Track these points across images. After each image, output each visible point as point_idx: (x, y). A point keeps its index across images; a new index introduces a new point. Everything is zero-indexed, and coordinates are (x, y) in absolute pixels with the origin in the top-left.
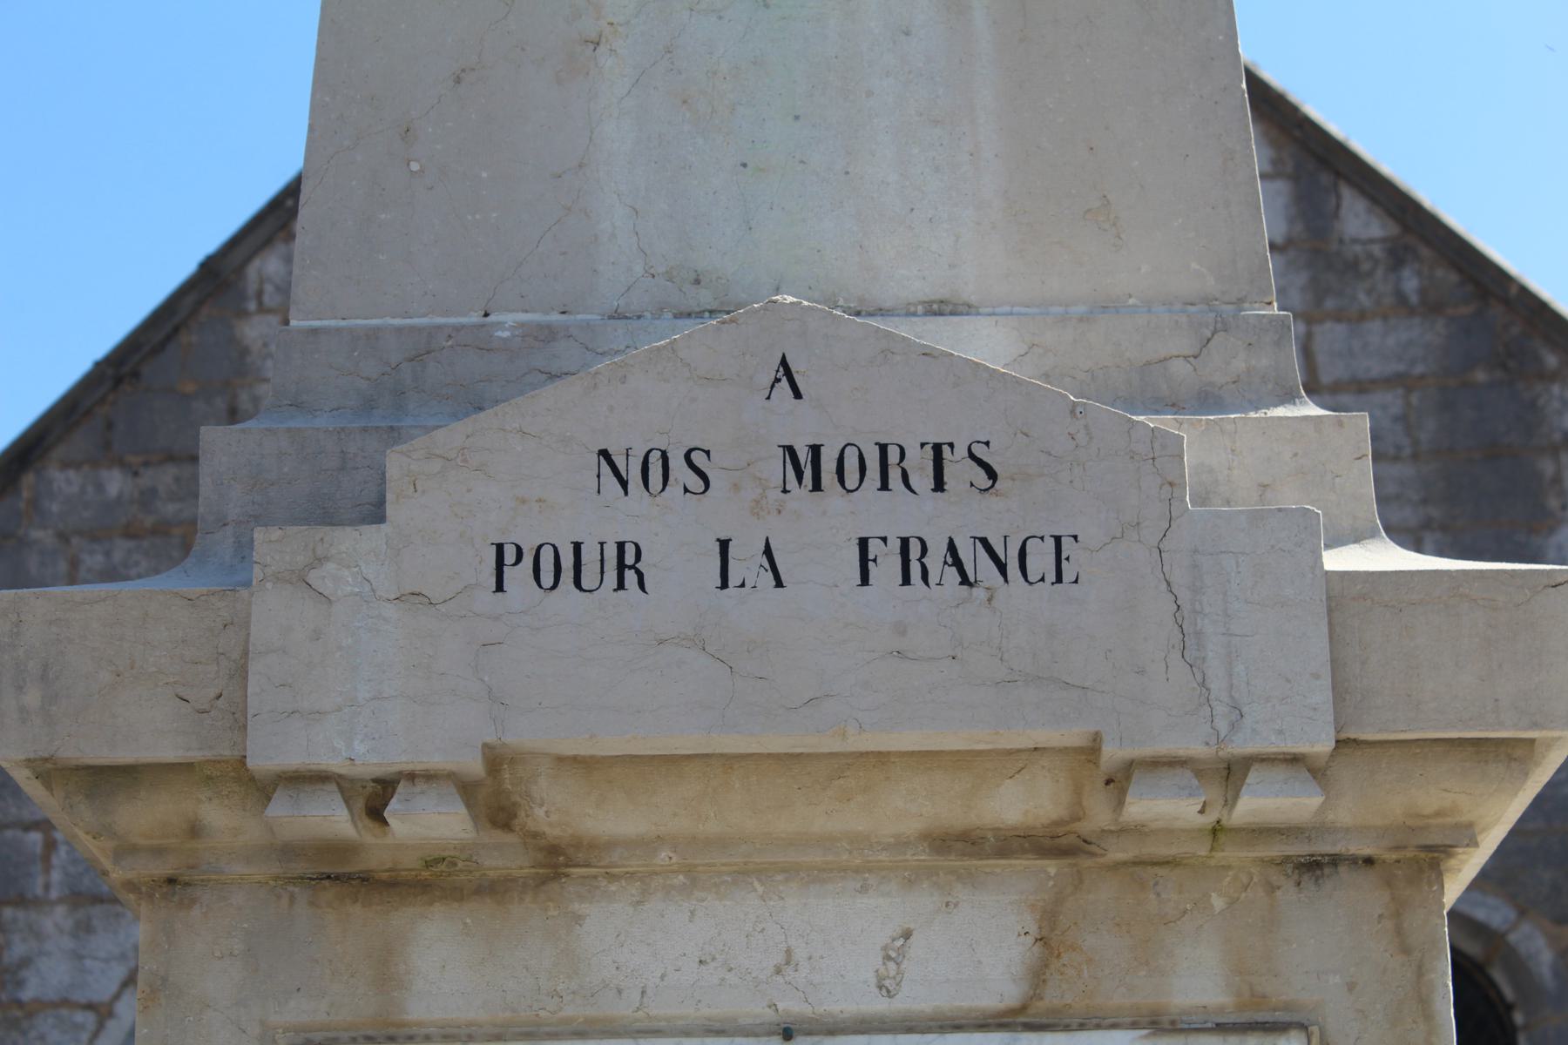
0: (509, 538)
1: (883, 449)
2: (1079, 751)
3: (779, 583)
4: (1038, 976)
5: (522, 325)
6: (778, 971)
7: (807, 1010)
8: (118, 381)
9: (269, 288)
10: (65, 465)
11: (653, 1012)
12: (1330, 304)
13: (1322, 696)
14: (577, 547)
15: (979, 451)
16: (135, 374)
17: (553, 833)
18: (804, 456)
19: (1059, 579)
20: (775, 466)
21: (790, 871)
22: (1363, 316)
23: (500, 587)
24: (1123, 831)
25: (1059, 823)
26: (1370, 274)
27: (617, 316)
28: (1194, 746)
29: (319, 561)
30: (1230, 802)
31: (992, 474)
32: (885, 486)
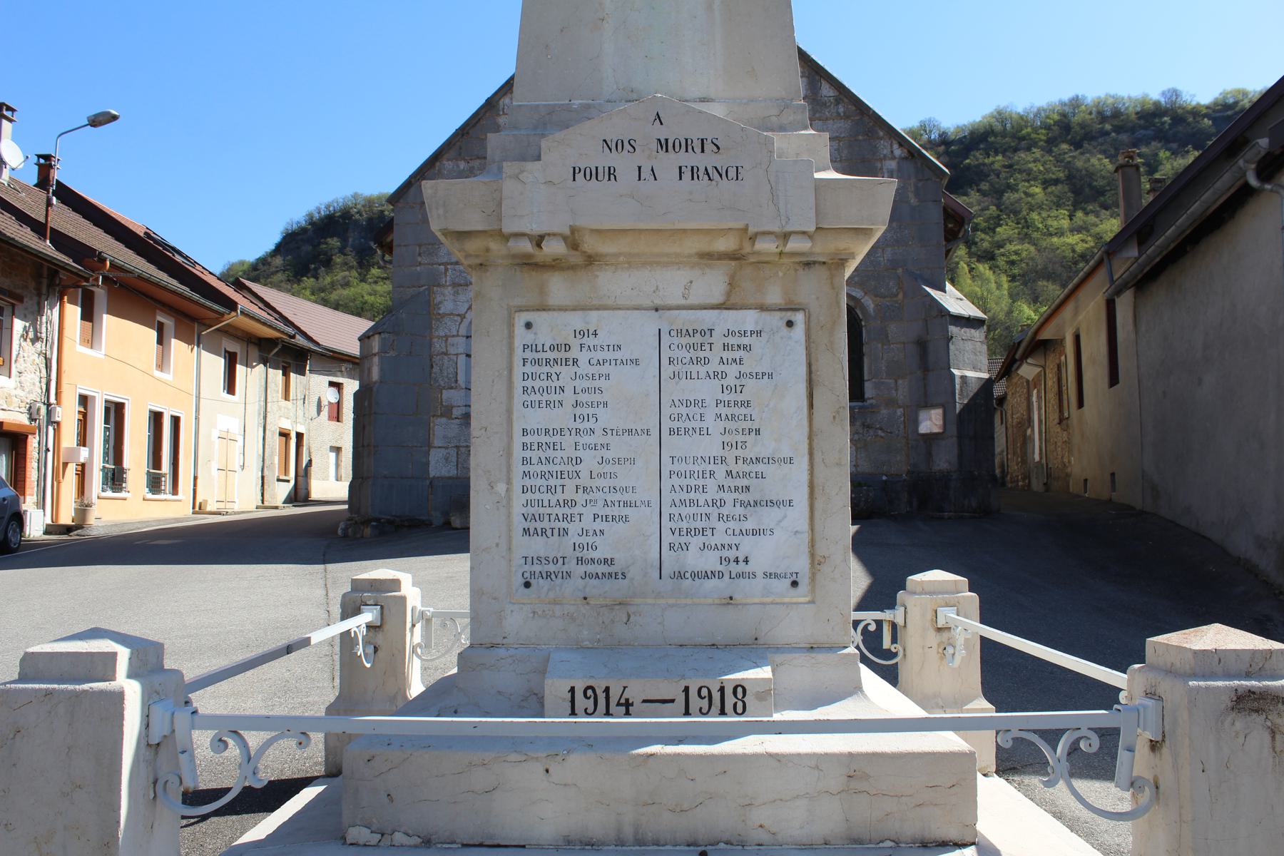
0: (577, 165)
1: (687, 140)
2: (742, 229)
3: (656, 179)
4: (729, 294)
5: (580, 104)
6: (654, 292)
7: (662, 303)
8: (463, 135)
10: (448, 160)
11: (619, 303)
12: (817, 115)
13: (812, 214)
14: (597, 168)
15: (715, 141)
16: (468, 133)
17: (589, 251)
18: (663, 142)
19: (737, 179)
20: (654, 145)
21: (658, 263)
22: (827, 119)
23: (574, 180)
24: (754, 253)
25: (735, 251)
26: (830, 106)
27: (609, 101)
28: (776, 229)
29: (522, 172)
30: (785, 245)
31: (718, 148)
32: (687, 151)
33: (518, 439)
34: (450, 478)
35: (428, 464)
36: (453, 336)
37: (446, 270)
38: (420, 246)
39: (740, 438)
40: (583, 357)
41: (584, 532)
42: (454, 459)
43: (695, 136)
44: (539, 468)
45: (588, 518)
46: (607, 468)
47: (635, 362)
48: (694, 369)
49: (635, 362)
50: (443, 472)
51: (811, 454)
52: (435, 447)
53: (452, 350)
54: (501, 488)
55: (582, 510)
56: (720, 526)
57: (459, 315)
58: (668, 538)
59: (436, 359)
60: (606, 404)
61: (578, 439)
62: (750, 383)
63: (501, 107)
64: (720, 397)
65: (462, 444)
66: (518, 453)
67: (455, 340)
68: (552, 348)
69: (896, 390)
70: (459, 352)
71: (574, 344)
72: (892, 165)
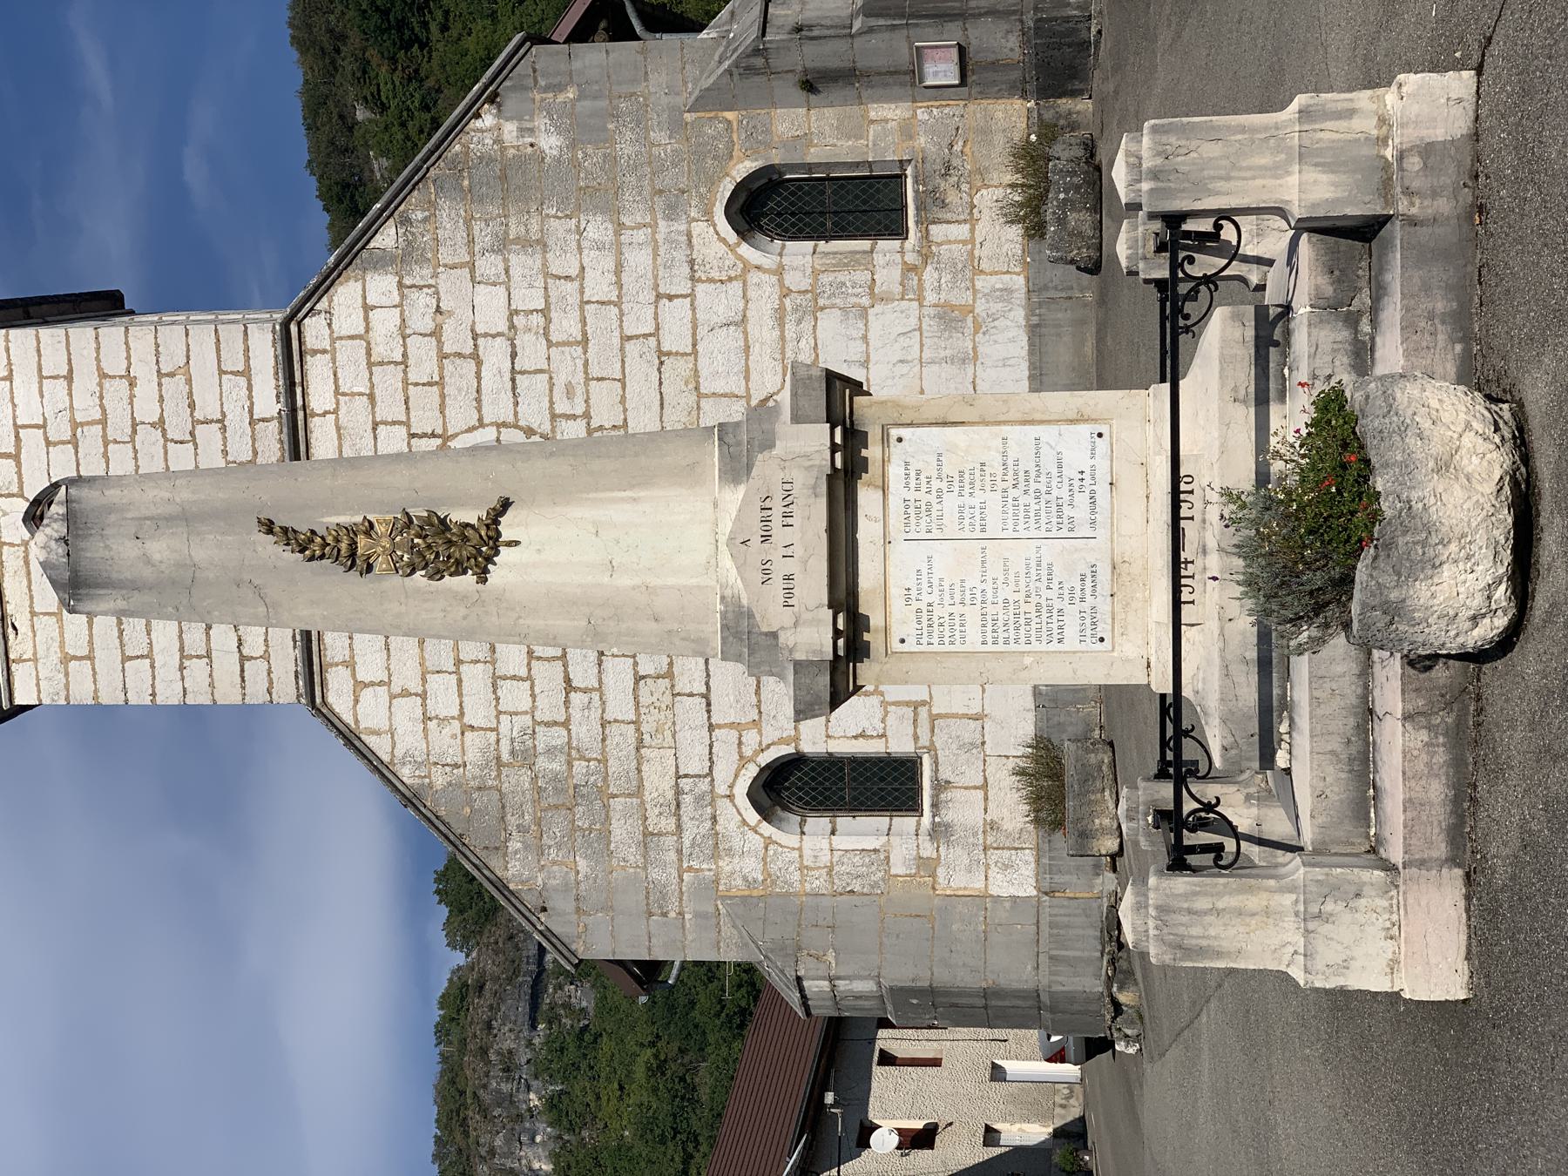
4: (876, 487)
9: (417, 773)
10: (506, 869)
20: (765, 545)
26: (413, 234)
33: (990, 647)
34: (1038, 862)
35: (1014, 899)
36: (801, 856)
37: (690, 869)
38: (651, 914)
39: (988, 478)
40: (926, 599)
41: (1061, 596)
42: (1006, 853)
43: (759, 515)
44: (1012, 631)
45: (1049, 594)
46: (1012, 578)
47: (930, 558)
48: (934, 513)
49: (930, 558)
50: (1027, 873)
51: (999, 423)
52: (986, 886)
53: (825, 859)
54: (1028, 660)
55: (1044, 598)
56: (1055, 493)
57: (766, 849)
58: (1064, 533)
59: (839, 884)
60: (963, 581)
61: (989, 602)
62: (946, 470)
63: (417, 781)
64: (956, 493)
65: (981, 841)
66: (1001, 647)
67: (807, 852)
68: (919, 623)
69: (886, 121)
70: (828, 846)
71: (915, 605)
72: (510, 129)
